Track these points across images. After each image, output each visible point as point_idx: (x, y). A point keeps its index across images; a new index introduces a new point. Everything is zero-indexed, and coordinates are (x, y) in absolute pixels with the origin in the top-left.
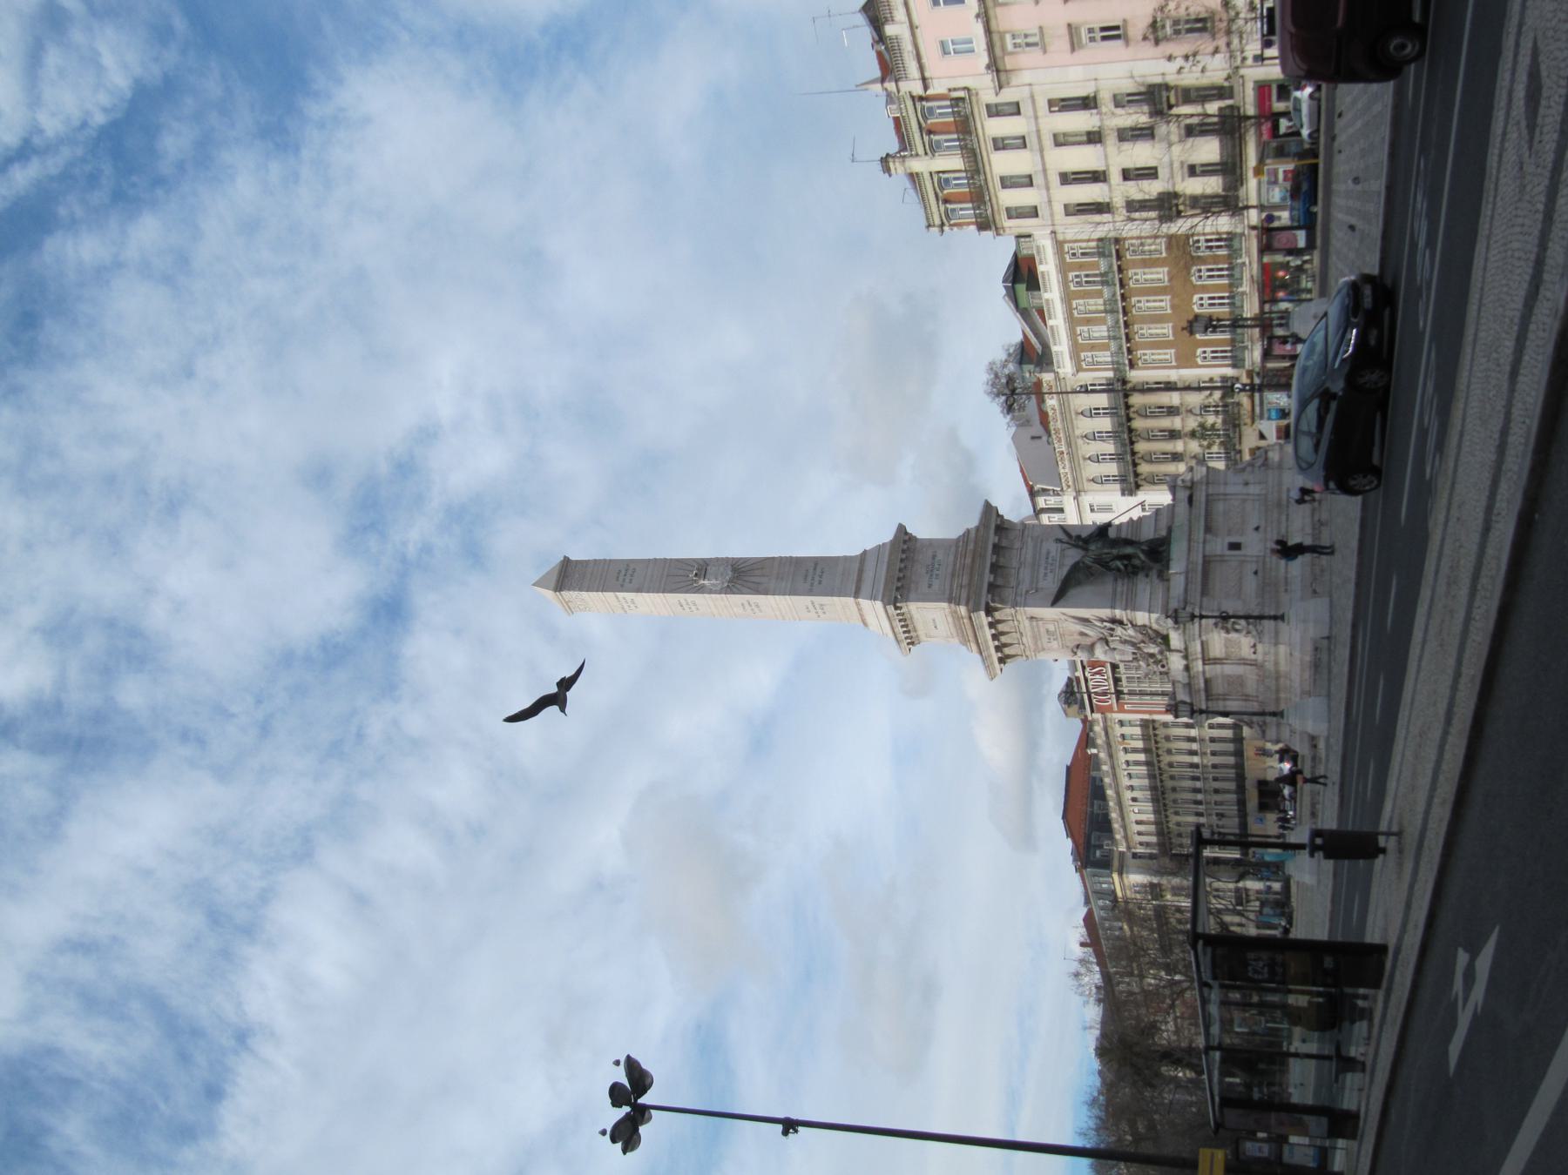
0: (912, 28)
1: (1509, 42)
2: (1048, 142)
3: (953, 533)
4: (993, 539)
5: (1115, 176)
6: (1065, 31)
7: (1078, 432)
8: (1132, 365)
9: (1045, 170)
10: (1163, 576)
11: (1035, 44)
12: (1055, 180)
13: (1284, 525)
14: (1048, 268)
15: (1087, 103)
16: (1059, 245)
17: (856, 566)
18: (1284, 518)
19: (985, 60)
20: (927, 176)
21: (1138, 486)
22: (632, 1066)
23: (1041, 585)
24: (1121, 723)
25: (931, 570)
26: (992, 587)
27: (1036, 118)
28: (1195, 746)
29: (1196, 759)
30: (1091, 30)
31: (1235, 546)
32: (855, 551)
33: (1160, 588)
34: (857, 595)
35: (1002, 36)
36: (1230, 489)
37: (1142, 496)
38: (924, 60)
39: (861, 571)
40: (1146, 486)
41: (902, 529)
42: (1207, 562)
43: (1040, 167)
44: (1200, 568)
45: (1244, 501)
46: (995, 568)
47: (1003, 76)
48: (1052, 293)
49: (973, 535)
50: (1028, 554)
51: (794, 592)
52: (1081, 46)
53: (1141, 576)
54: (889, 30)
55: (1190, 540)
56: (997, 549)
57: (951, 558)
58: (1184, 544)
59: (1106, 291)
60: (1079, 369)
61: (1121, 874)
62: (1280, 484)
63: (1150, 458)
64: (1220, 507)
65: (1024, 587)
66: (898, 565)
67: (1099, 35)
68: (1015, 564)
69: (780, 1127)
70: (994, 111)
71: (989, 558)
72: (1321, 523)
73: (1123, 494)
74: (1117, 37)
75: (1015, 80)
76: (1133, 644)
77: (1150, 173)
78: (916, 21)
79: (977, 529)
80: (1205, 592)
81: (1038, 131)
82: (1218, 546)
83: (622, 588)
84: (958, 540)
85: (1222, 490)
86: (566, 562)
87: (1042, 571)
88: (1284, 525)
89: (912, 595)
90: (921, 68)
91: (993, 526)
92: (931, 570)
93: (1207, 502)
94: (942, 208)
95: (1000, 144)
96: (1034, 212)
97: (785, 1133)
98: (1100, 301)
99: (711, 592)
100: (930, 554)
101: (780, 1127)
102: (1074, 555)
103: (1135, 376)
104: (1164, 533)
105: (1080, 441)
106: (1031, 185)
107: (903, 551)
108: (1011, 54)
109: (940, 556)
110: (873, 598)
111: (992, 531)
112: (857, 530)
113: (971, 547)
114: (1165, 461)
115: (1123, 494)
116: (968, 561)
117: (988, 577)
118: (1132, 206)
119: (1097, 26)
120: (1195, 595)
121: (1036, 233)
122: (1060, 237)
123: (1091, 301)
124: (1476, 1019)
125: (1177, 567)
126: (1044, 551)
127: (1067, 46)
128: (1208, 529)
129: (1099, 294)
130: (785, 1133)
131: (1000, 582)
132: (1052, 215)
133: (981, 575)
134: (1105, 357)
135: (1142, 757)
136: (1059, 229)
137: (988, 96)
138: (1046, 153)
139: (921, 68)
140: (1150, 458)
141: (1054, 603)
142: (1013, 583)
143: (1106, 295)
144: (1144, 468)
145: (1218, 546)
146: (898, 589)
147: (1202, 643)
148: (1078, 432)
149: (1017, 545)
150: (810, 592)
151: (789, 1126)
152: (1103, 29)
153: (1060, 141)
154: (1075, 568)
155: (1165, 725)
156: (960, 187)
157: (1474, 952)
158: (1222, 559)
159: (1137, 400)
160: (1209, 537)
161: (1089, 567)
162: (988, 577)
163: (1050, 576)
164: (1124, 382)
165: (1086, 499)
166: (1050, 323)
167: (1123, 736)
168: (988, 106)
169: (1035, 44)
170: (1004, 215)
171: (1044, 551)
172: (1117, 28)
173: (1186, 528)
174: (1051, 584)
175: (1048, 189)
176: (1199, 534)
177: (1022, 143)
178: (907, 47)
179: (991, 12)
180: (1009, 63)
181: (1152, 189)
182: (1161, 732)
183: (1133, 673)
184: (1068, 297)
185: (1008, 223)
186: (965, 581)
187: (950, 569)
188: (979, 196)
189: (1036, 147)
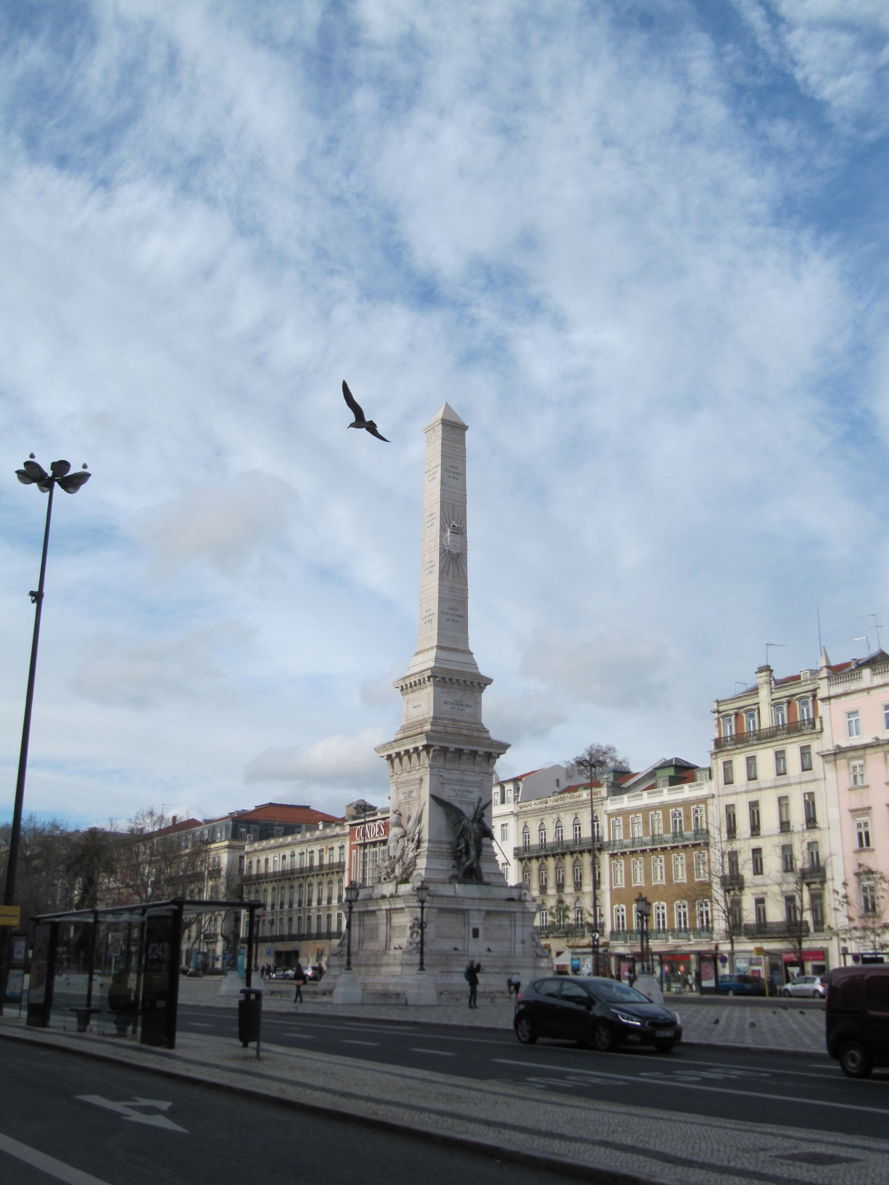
0: (868, 690)
1: (857, 1140)
2: (782, 792)
3: (486, 720)
4: (482, 750)
5: (755, 843)
6: (865, 804)
7: (562, 815)
8: (613, 855)
9: (760, 789)
10: (453, 879)
11: (855, 782)
12: (753, 797)
13: (492, 970)
14: (686, 792)
15: (811, 822)
16: (704, 800)
17: (460, 647)
18: (497, 970)
19: (844, 744)
20: (756, 700)
21: (521, 860)
22: (81, 478)
23: (446, 786)
24: (342, 848)
25: (458, 703)
26: (445, 750)
27: (800, 783)
28: (324, 903)
29: (314, 904)
30: (866, 824)
31: (476, 933)
32: (472, 648)
33: (445, 876)
34: (439, 647)
35: (862, 757)
36: (519, 930)
37: (514, 862)
38: (843, 699)
40: (521, 866)
41: (489, 681)
42: (464, 912)
43: (762, 786)
44: (459, 907)
45: (510, 941)
46: (459, 752)
47: (831, 758)
48: (667, 795)
49: (484, 735)
50: (470, 777)
51: (441, 600)
52: (854, 817)
53: (453, 862)
54: (866, 672)
55: (480, 899)
56: (474, 754)
57: (467, 719)
58: (477, 895)
59: (668, 836)
60: (610, 815)
61: (228, 847)
62: (523, 967)
63: (542, 869)
64: (506, 922)
65: (445, 774)
66: (461, 679)
67: (863, 830)
68: (462, 767)
69: (36, 589)
70: (805, 751)
71: (467, 748)
72: (493, 999)
73: (515, 849)
74: (861, 845)
75: (828, 767)
76: (401, 857)
77: (758, 869)
78: (873, 692)
79: (489, 739)
80: (442, 911)
81: (790, 785)
82: (476, 921)
83: (444, 470)
84: (480, 724)
85: (518, 923)
86: (464, 428)
87: (457, 788)
88: (492, 970)
89: (439, 689)
90: (837, 696)
91: (491, 750)
92: (458, 703)
93: (509, 913)
94: (731, 712)
95: (780, 756)
96: (728, 781)
97: (32, 594)
98: (661, 832)
99: (441, 537)
101: (36, 589)
102: (469, 811)
103: (605, 859)
104: (486, 879)
105: (555, 816)
106: (750, 779)
107: (472, 683)
108: (849, 764)
109: (468, 710)
110: (437, 660)
111: (487, 750)
112: (487, 649)
113: (475, 734)
114: (540, 881)
115: (515, 849)
116: (465, 732)
117: (452, 747)
118: (733, 856)
119: (869, 829)
120: (438, 903)
121: (712, 783)
122: (710, 801)
123: (661, 825)
124: (118, 1115)
125: (460, 889)
126: (472, 789)
127: (855, 806)
128: (489, 913)
129: (667, 831)
130: (32, 594)
131: (449, 756)
132: (727, 795)
133: (453, 742)
134: (619, 835)
135: (316, 863)
136: (715, 801)
137: (817, 747)
138: (773, 790)
139: (837, 696)
140: (542, 869)
141: (433, 797)
142: (448, 766)
143: (666, 836)
144: (535, 865)
145: (476, 921)
146: (444, 678)
147: (402, 909)
148: (562, 815)
149: (477, 769)
150: (441, 612)
151: (37, 597)
152: (867, 834)
153: (783, 801)
154: (459, 812)
155: (341, 881)
156: (748, 726)
157: (169, 1114)
158: (466, 923)
159: (587, 859)
160: (483, 913)
161: (460, 823)
162: (452, 747)
163: (453, 794)
164: (600, 850)
165: (511, 821)
166: (645, 794)
167: (332, 849)
168: (809, 747)
169: (855, 782)
170: (726, 759)
171: (472, 789)
172: (868, 844)
173: (489, 896)
174: (447, 795)
175: (746, 792)
176: (485, 906)
177: (781, 772)
178: (854, 686)
179: (880, 749)
180: (842, 762)
181: (746, 870)
182: (335, 878)
183: (380, 856)
184: (664, 807)
185: (720, 762)
186: (449, 729)
187: (458, 718)
188: (741, 740)
189: (778, 783)
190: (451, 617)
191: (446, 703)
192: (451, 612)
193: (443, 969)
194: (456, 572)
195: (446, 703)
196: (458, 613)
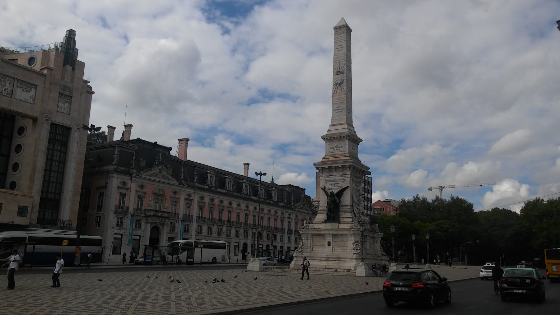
4: (340, 165)
39: (339, 125)
42: (324, 235)
46: (330, 168)
56: (337, 168)
57: (341, 153)
62: (347, 258)
65: (328, 179)
68: (334, 174)
80: (313, 235)
89: (328, 143)
92: (337, 147)
100: (343, 145)
113: (342, 158)
116: (337, 159)
117: (326, 166)
128: (335, 236)
149: (341, 173)
162: (326, 166)
163: (331, 186)
186: (330, 159)
194: (340, 91)
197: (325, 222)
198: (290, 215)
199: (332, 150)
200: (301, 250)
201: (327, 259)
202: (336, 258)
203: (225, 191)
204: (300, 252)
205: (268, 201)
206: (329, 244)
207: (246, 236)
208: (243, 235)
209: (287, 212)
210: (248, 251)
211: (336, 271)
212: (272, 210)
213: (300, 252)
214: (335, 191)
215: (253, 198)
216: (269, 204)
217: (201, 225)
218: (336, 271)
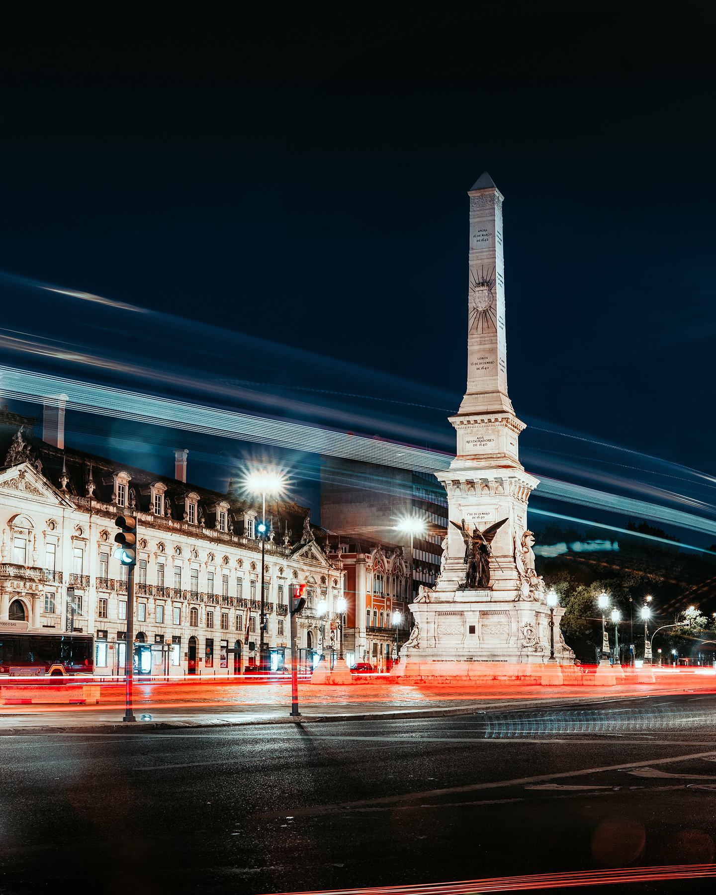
25: (481, 440)
31: (472, 630)
64: (503, 619)
65: (462, 502)
82: (472, 619)
117: (462, 479)
125: (460, 596)
128: (484, 614)
131: (461, 486)
158: (464, 622)
190: (481, 366)
191: (468, 442)
192: (481, 361)
193: (435, 659)
194: (485, 325)
195: (468, 442)
196: (487, 361)
197: (462, 588)
198: (281, 570)
199: (471, 444)
200: (415, 643)
201: (470, 659)
202: (488, 656)
203: (150, 518)
204: (414, 647)
205: (235, 539)
206: (472, 630)
207: (194, 623)
208: (189, 619)
209: (275, 564)
210: (200, 656)
211: (495, 679)
212: (244, 559)
213: (414, 647)
214: (482, 529)
215: (207, 532)
216: (240, 545)
217: (106, 596)
218: (495, 679)
